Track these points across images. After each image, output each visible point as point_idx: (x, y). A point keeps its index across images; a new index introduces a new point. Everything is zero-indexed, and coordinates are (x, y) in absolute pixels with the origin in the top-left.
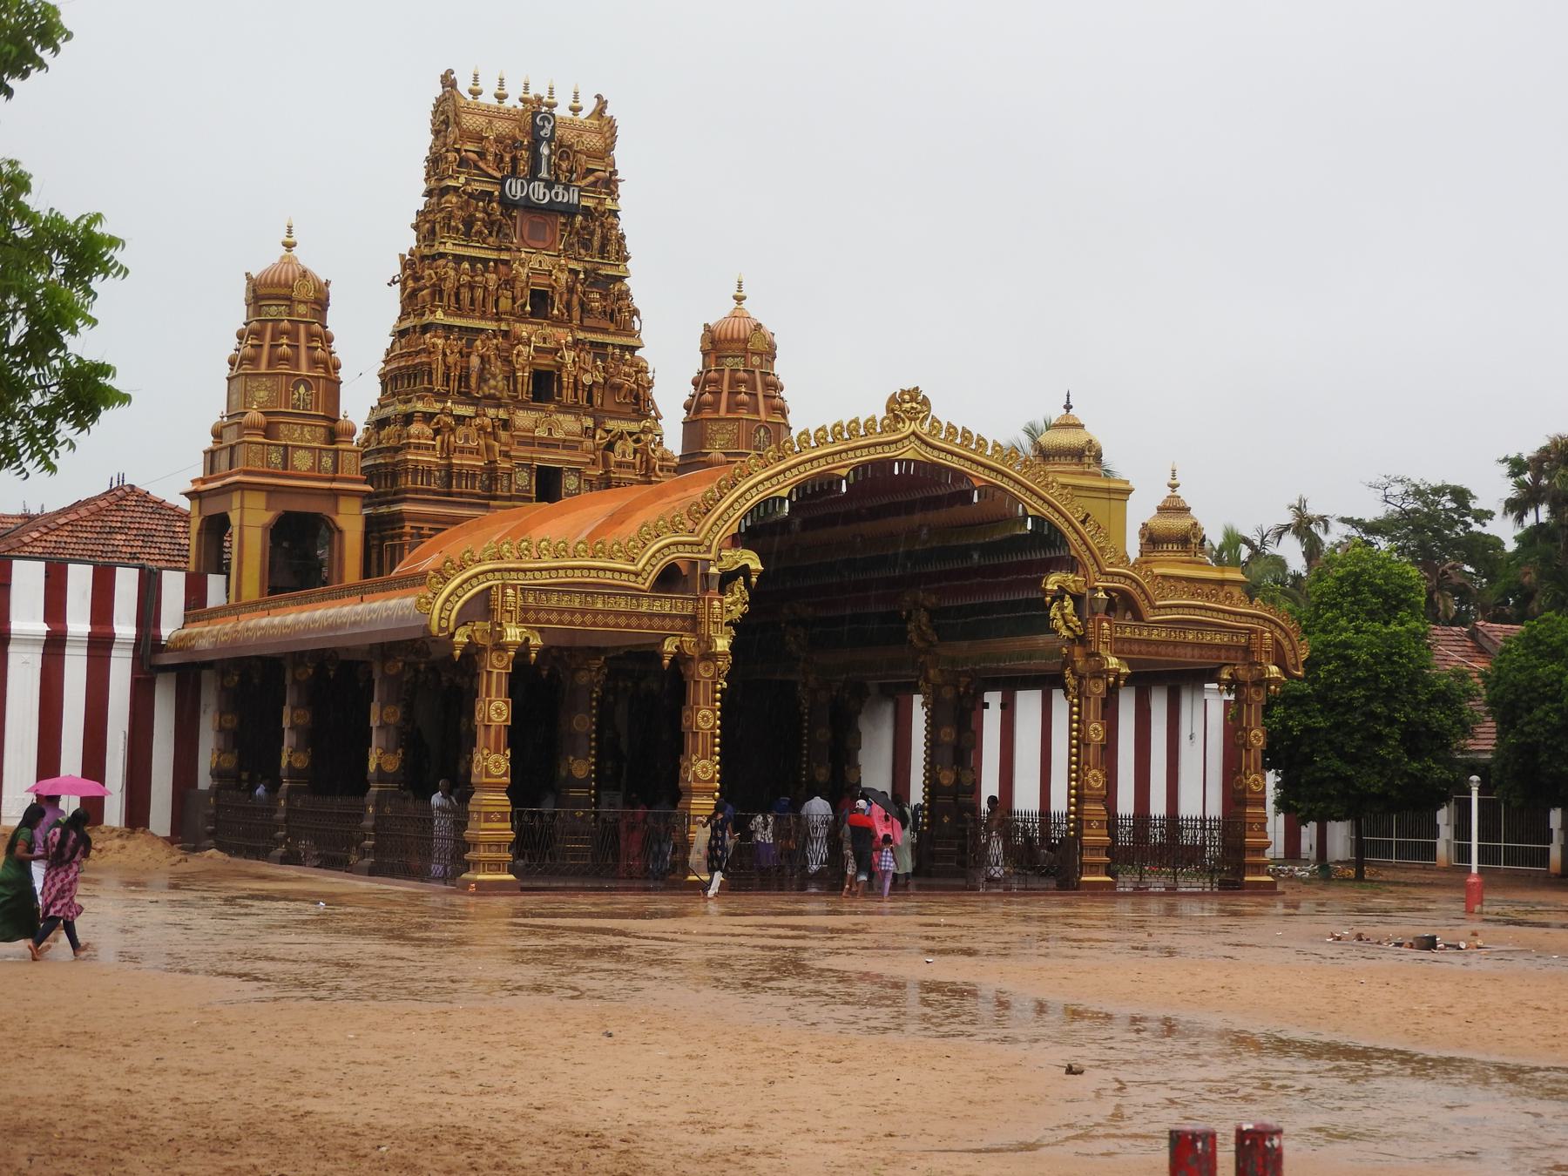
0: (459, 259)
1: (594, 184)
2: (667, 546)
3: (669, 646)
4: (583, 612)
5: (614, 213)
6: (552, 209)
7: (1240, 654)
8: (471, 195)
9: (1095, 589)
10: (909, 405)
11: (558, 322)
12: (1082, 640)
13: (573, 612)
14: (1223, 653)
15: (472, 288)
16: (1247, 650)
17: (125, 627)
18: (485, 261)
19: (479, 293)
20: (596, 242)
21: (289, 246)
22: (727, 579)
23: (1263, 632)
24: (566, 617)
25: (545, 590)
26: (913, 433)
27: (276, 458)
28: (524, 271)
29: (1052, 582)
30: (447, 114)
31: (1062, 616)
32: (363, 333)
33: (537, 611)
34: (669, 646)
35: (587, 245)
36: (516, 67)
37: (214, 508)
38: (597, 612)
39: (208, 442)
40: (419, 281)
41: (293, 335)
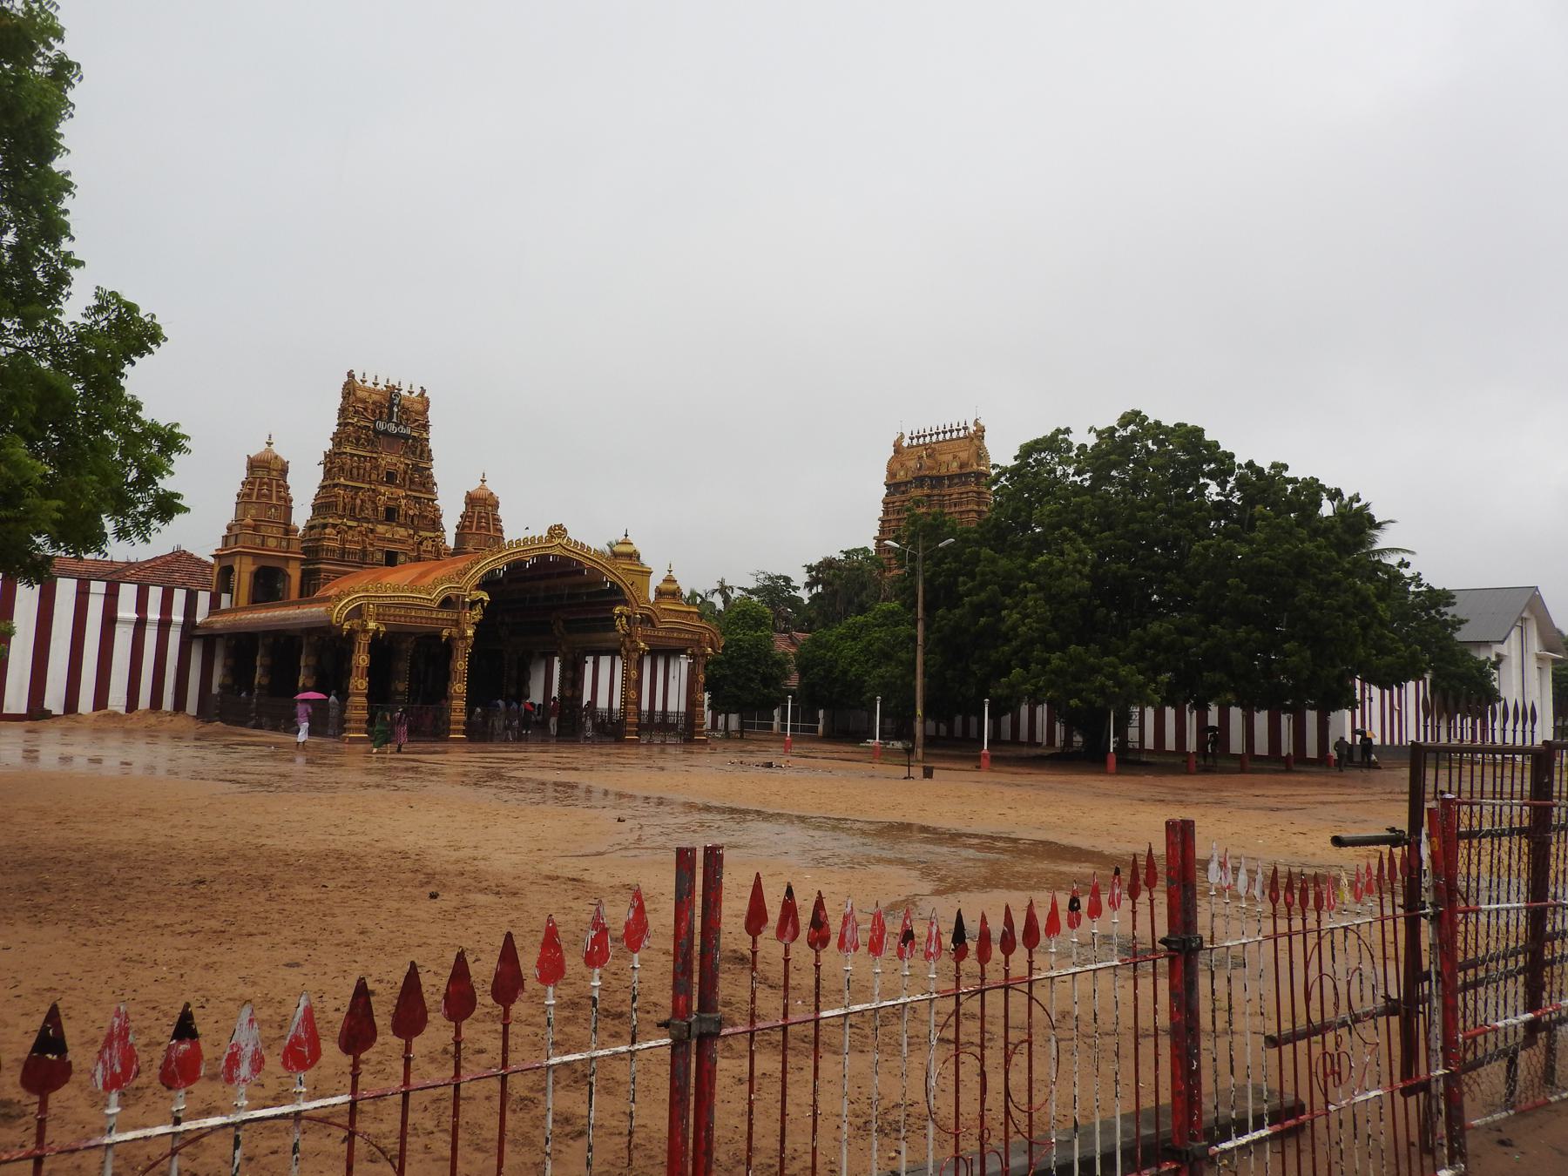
0: (352, 455)
3: (445, 633)
6: (398, 435)
10: (557, 531)
11: (398, 486)
12: (629, 635)
17: (178, 617)
21: (269, 444)
22: (473, 604)
25: (388, 606)
27: (258, 541)
29: (617, 610)
30: (350, 389)
31: (621, 624)
32: (304, 487)
34: (445, 633)
36: (385, 369)
37: (226, 563)
39: (225, 532)
40: (332, 463)
41: (270, 485)
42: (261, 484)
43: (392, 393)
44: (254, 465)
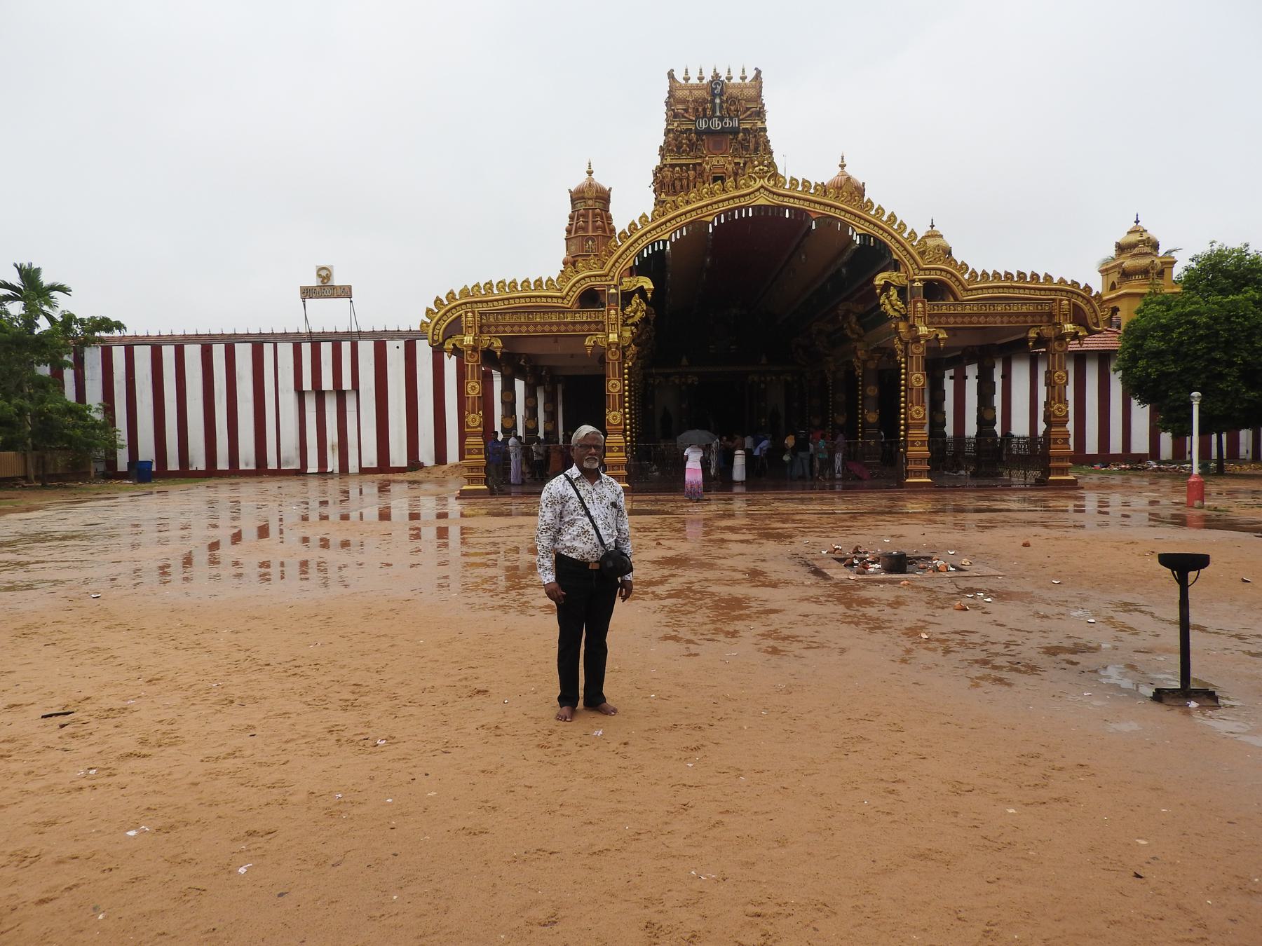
1: (750, 115)
2: (583, 278)
4: (528, 325)
5: (765, 130)
6: (723, 132)
7: (1045, 318)
8: (681, 132)
9: (914, 281)
13: (520, 325)
14: (1029, 319)
15: (681, 180)
16: (1051, 315)
18: (687, 165)
19: (685, 182)
20: (752, 147)
21: (590, 173)
22: (627, 297)
23: (1061, 300)
24: (516, 328)
26: (762, 187)
28: (707, 168)
29: (880, 280)
33: (497, 326)
35: (747, 149)
36: (703, 61)
38: (536, 324)
42: (595, 215)
43: (717, 86)
44: (577, 197)
